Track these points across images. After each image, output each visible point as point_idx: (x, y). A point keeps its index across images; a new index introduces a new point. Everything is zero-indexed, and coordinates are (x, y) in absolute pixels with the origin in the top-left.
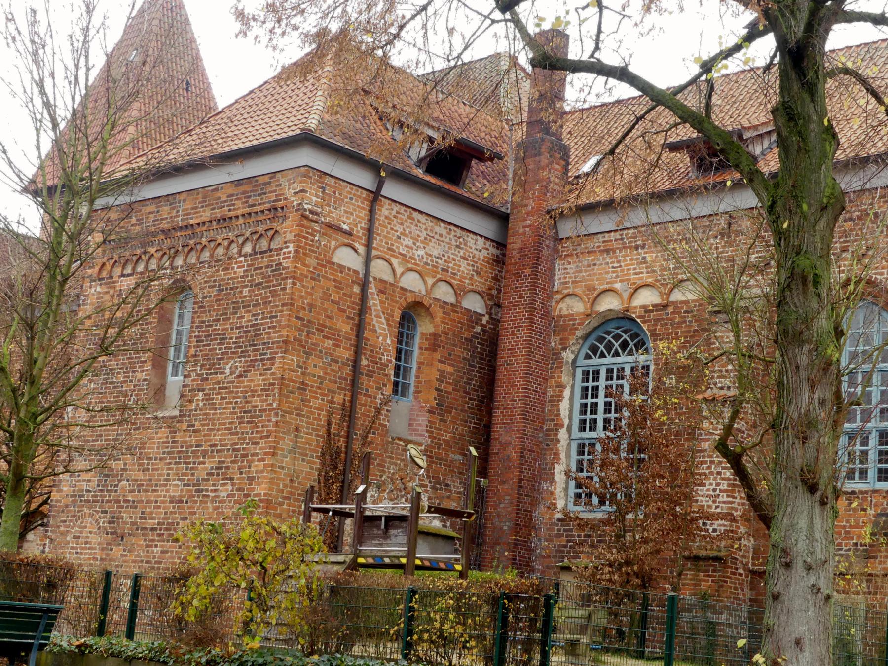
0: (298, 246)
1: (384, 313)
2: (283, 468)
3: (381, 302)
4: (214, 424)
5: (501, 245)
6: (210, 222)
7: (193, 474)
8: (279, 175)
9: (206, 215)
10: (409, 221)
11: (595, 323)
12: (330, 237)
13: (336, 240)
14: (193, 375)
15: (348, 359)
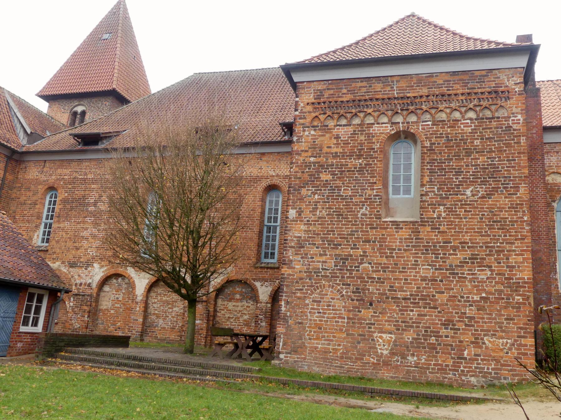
7: (445, 262)
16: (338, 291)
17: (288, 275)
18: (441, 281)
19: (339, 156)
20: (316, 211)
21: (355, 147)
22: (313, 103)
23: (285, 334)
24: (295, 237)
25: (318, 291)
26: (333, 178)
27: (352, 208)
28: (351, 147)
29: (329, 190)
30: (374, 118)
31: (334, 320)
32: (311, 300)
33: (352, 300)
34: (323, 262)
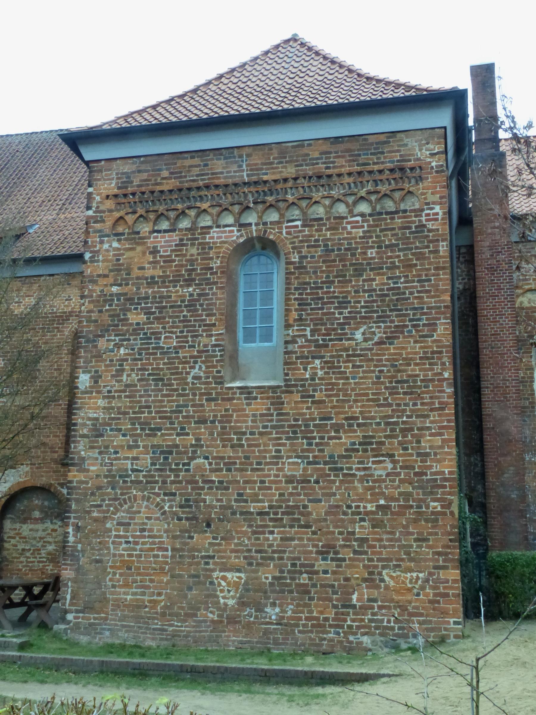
7: (322, 451)
16: (158, 504)
17: (78, 482)
18: (317, 482)
19: (157, 282)
20: (122, 376)
21: (182, 266)
22: (116, 196)
23: (75, 581)
24: (89, 419)
25: (126, 507)
26: (148, 318)
27: (178, 368)
28: (176, 266)
29: (141, 339)
30: (212, 217)
31: (152, 553)
32: (115, 522)
33: (180, 519)
34: (134, 459)
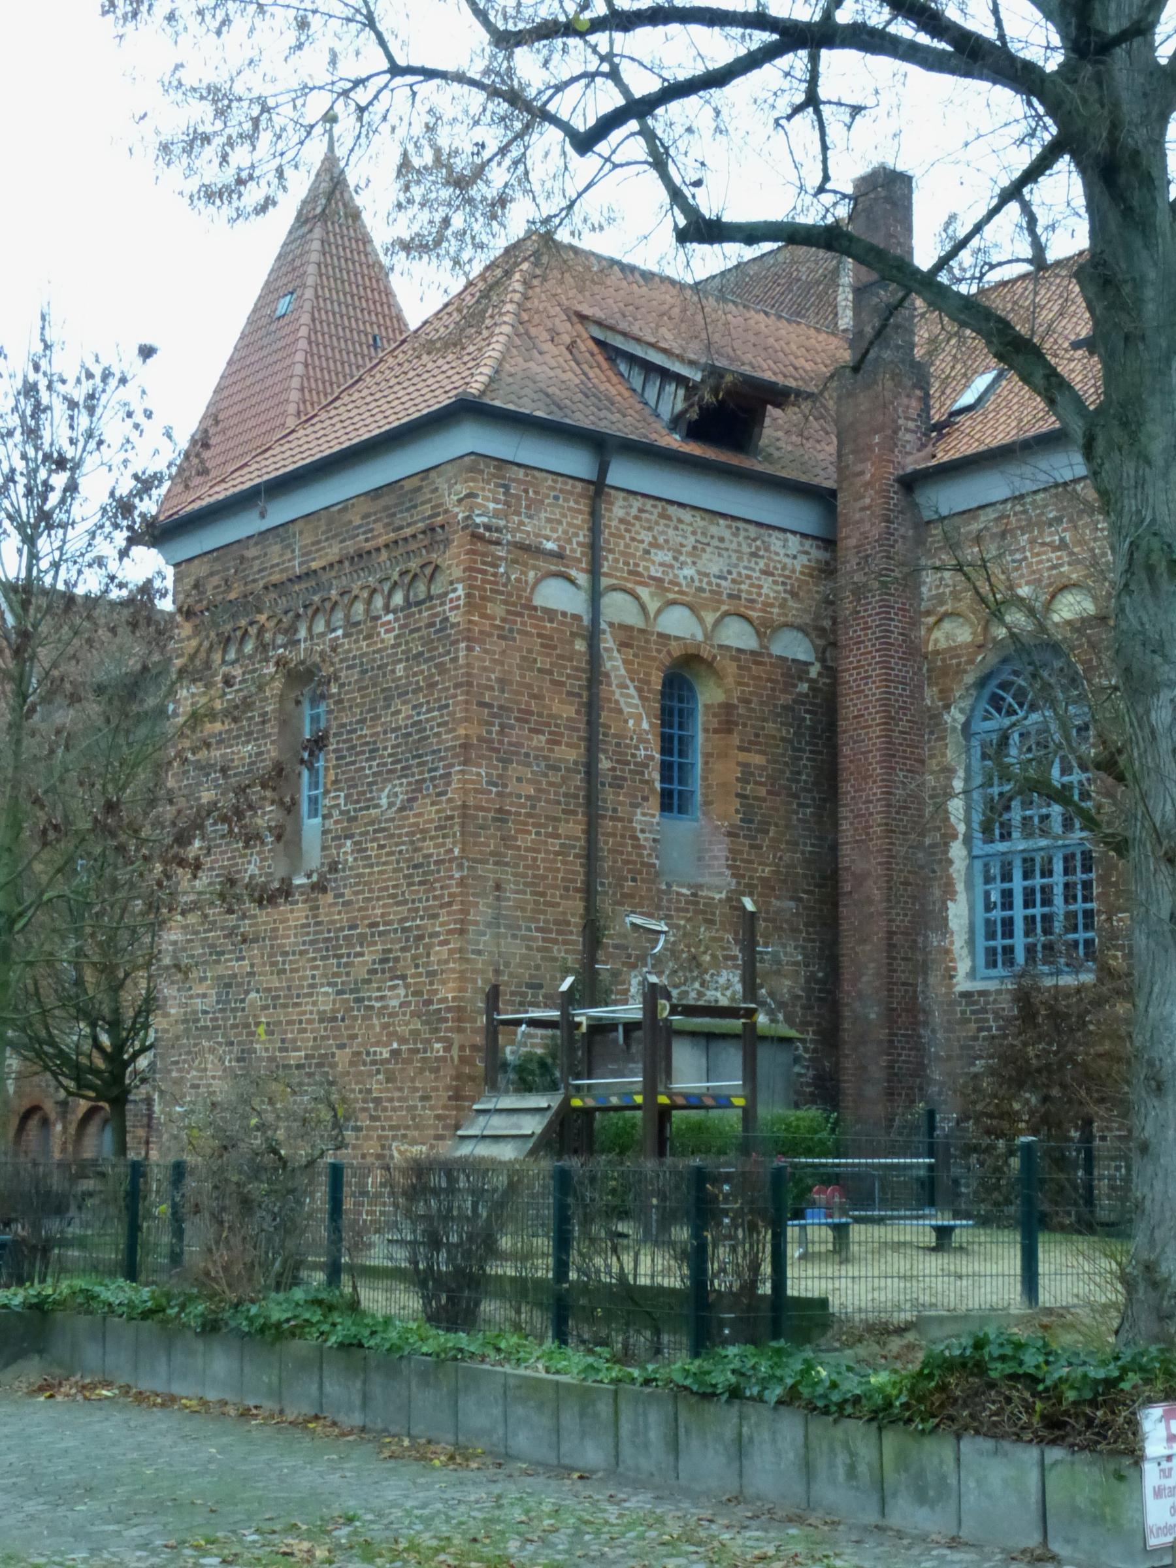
0: (471, 587)
1: (632, 680)
2: (479, 953)
3: (625, 662)
4: (371, 891)
5: (829, 543)
6: (340, 562)
7: (348, 974)
8: (433, 474)
9: (333, 552)
10: (662, 522)
11: (993, 659)
12: (525, 565)
13: (535, 568)
14: (336, 813)
15: (576, 763)
18: (343, 1020)
